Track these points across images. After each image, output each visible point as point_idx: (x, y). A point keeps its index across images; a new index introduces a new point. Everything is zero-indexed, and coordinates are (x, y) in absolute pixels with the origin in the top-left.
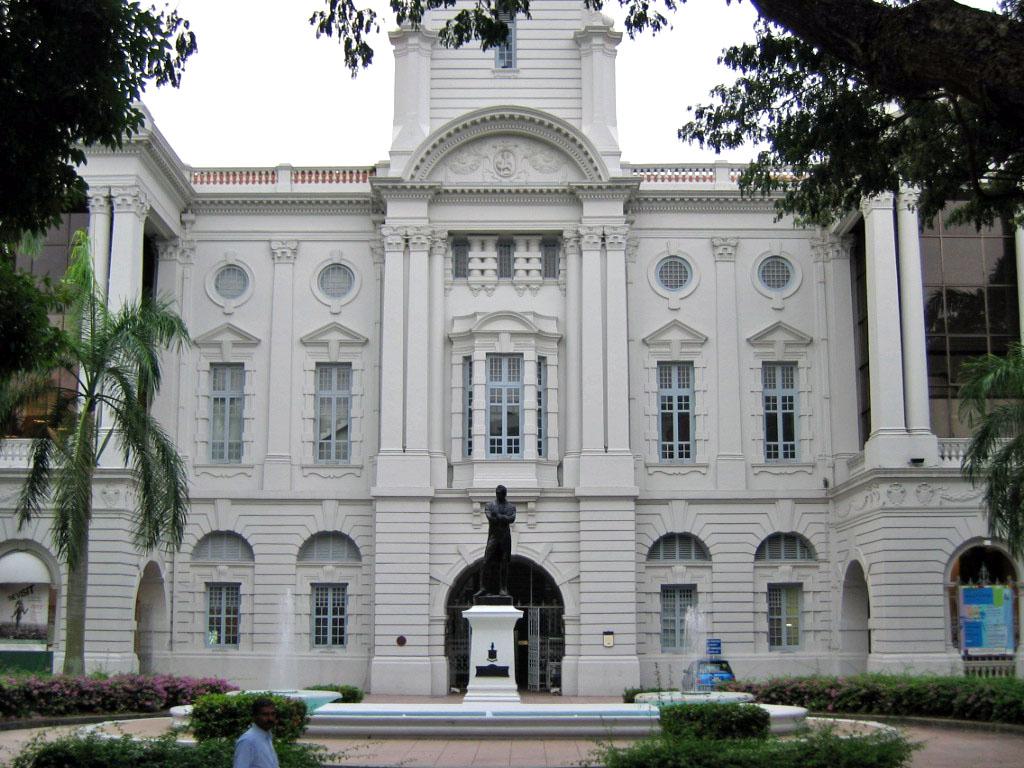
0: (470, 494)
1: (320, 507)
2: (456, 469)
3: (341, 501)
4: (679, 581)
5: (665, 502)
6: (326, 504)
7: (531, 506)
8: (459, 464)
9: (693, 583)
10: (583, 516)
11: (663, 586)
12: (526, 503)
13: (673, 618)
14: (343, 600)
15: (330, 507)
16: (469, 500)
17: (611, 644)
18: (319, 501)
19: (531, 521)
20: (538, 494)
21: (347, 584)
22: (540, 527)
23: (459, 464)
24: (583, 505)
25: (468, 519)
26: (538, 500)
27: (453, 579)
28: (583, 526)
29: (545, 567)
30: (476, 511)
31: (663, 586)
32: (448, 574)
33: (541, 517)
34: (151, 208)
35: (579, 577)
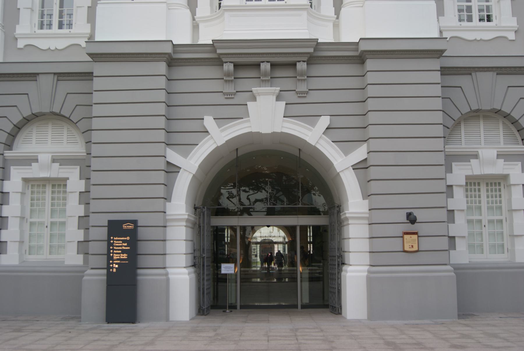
0: (219, 51)
1: (34, 82)
2: (201, 26)
3: (61, 76)
4: (489, 171)
5: (468, 71)
6: (41, 78)
7: (302, 66)
8: (206, 20)
9: (505, 172)
10: (371, 78)
11: (467, 178)
12: (293, 65)
13: (479, 218)
14: (65, 199)
15: (46, 82)
16: (218, 61)
17: (415, 248)
18: (33, 76)
19: (302, 87)
20: (311, 50)
21: (68, 179)
22: (314, 96)
23: (206, 20)
24: (370, 64)
25: (217, 86)
26: (312, 60)
27: (197, 165)
28: (371, 91)
29: (318, 146)
30: (228, 75)
31: (467, 178)
32: (196, 162)
33: (315, 83)
34: (90, 55)
35: (366, 159)
